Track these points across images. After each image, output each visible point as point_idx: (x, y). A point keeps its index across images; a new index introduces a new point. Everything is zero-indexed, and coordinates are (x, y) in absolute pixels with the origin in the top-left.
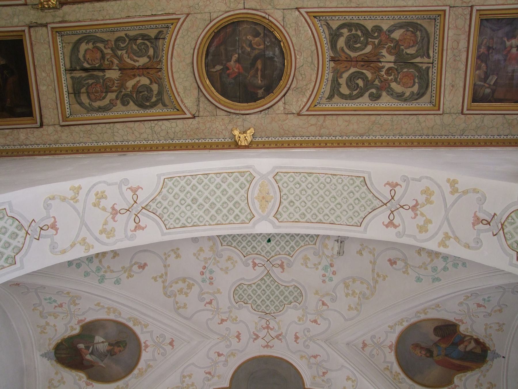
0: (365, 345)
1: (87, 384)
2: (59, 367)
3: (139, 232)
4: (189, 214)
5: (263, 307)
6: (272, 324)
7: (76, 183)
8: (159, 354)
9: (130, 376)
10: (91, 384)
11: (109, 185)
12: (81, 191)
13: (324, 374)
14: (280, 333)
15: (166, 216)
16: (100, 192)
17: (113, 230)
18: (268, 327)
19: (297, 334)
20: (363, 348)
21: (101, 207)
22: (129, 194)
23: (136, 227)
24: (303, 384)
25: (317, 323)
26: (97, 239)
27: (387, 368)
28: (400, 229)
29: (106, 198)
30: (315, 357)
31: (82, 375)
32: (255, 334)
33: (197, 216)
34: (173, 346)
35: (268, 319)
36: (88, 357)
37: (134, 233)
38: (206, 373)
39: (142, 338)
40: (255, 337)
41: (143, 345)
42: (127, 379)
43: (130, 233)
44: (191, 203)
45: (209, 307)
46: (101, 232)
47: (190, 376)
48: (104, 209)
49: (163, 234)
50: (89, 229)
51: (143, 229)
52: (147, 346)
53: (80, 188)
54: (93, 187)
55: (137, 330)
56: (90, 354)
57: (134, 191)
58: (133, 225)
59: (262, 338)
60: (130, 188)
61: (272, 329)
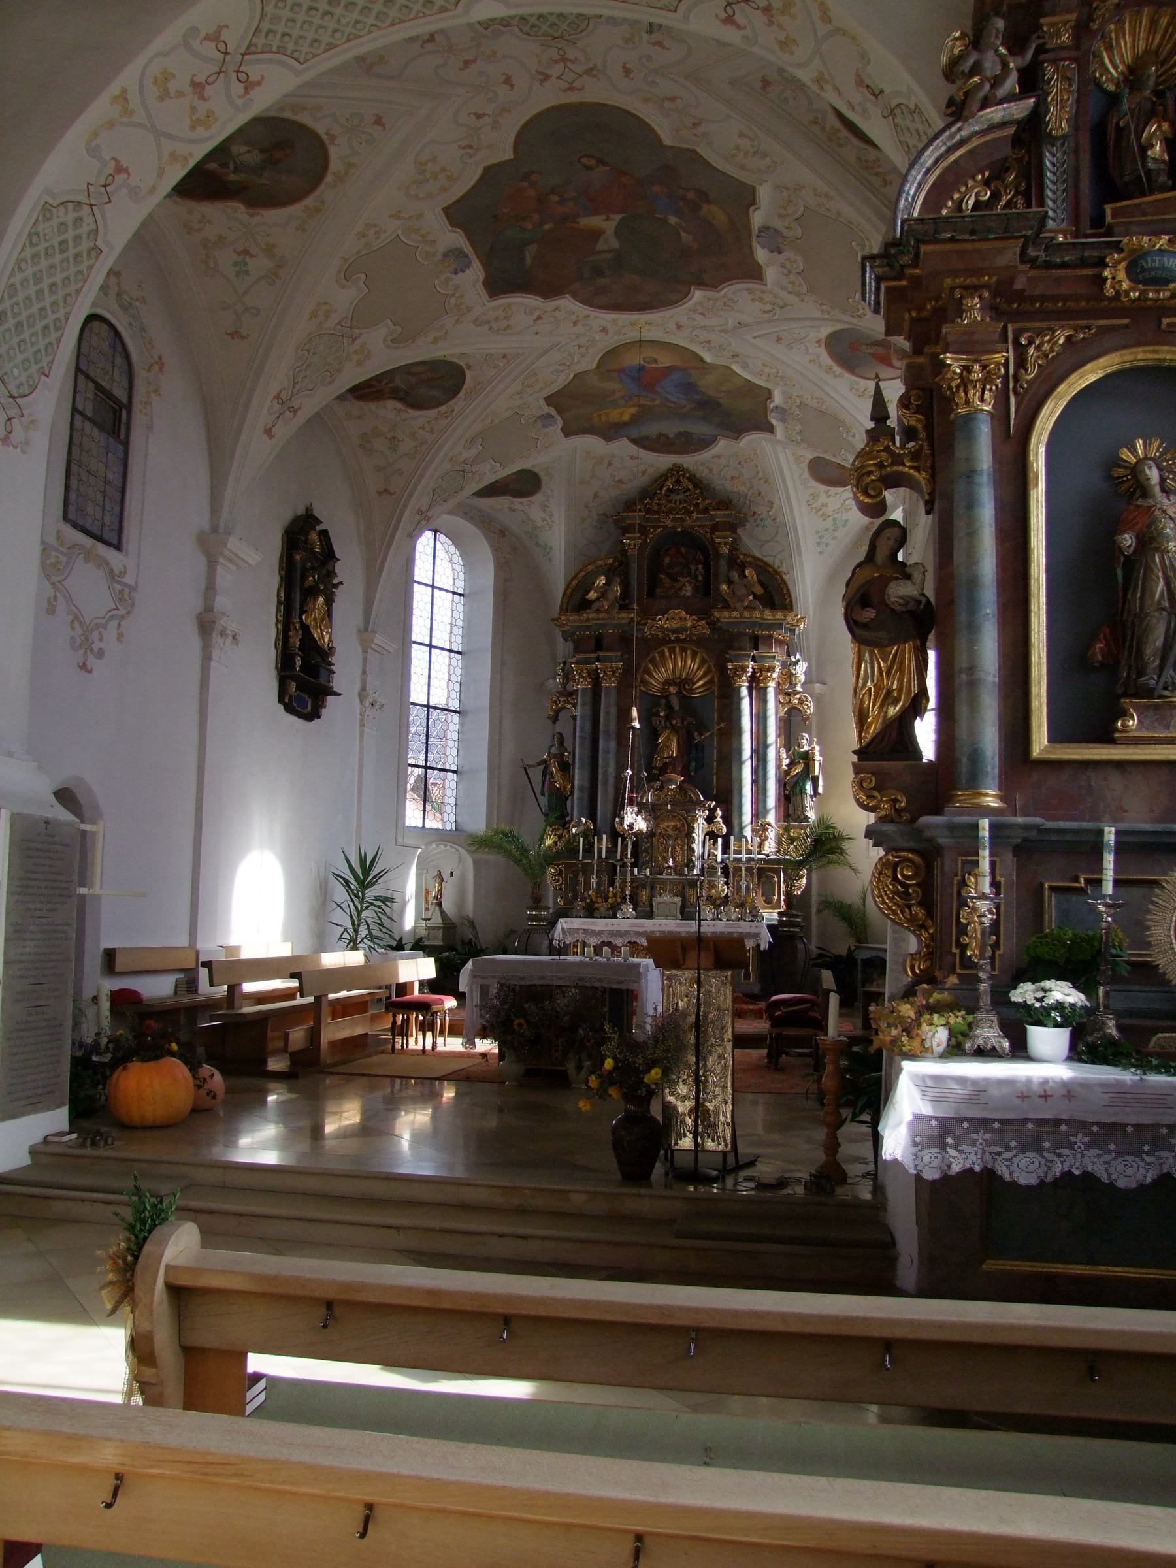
0: (766, 83)
1: (252, 216)
2: (193, 204)
3: (256, 93)
4: (332, 25)
5: (545, 27)
6: (571, 53)
7: (115, 89)
8: (361, 143)
9: (322, 187)
10: (258, 214)
11: (166, 54)
12: (129, 97)
13: (695, 125)
14: (591, 65)
15: (291, 47)
16: (158, 75)
17: (210, 114)
18: (564, 60)
19: (628, 66)
20: (764, 88)
21: (172, 94)
22: (209, 50)
23: (246, 88)
24: (660, 140)
25: (664, 47)
26: (191, 141)
27: (815, 122)
28: (748, 32)
29: (173, 76)
30: (673, 99)
31: (236, 204)
32: (541, 73)
33: (348, 23)
34: (383, 125)
35: (560, 46)
36: (232, 177)
37: (248, 97)
38: (463, 148)
39: (320, 128)
40: (541, 77)
41: (325, 137)
42: (317, 193)
43: (239, 102)
44: (328, 8)
45: (429, 46)
46: (193, 128)
47: (434, 160)
48: (180, 94)
49: (297, 74)
50: (170, 136)
51: (259, 83)
52: (333, 138)
53: (124, 91)
54: (143, 74)
55: (304, 118)
56: (234, 172)
57: (215, 37)
58: (239, 88)
59: (558, 78)
60: (205, 39)
61: (572, 62)
